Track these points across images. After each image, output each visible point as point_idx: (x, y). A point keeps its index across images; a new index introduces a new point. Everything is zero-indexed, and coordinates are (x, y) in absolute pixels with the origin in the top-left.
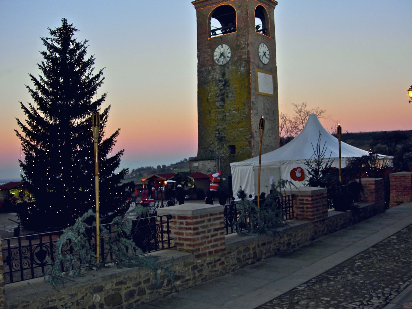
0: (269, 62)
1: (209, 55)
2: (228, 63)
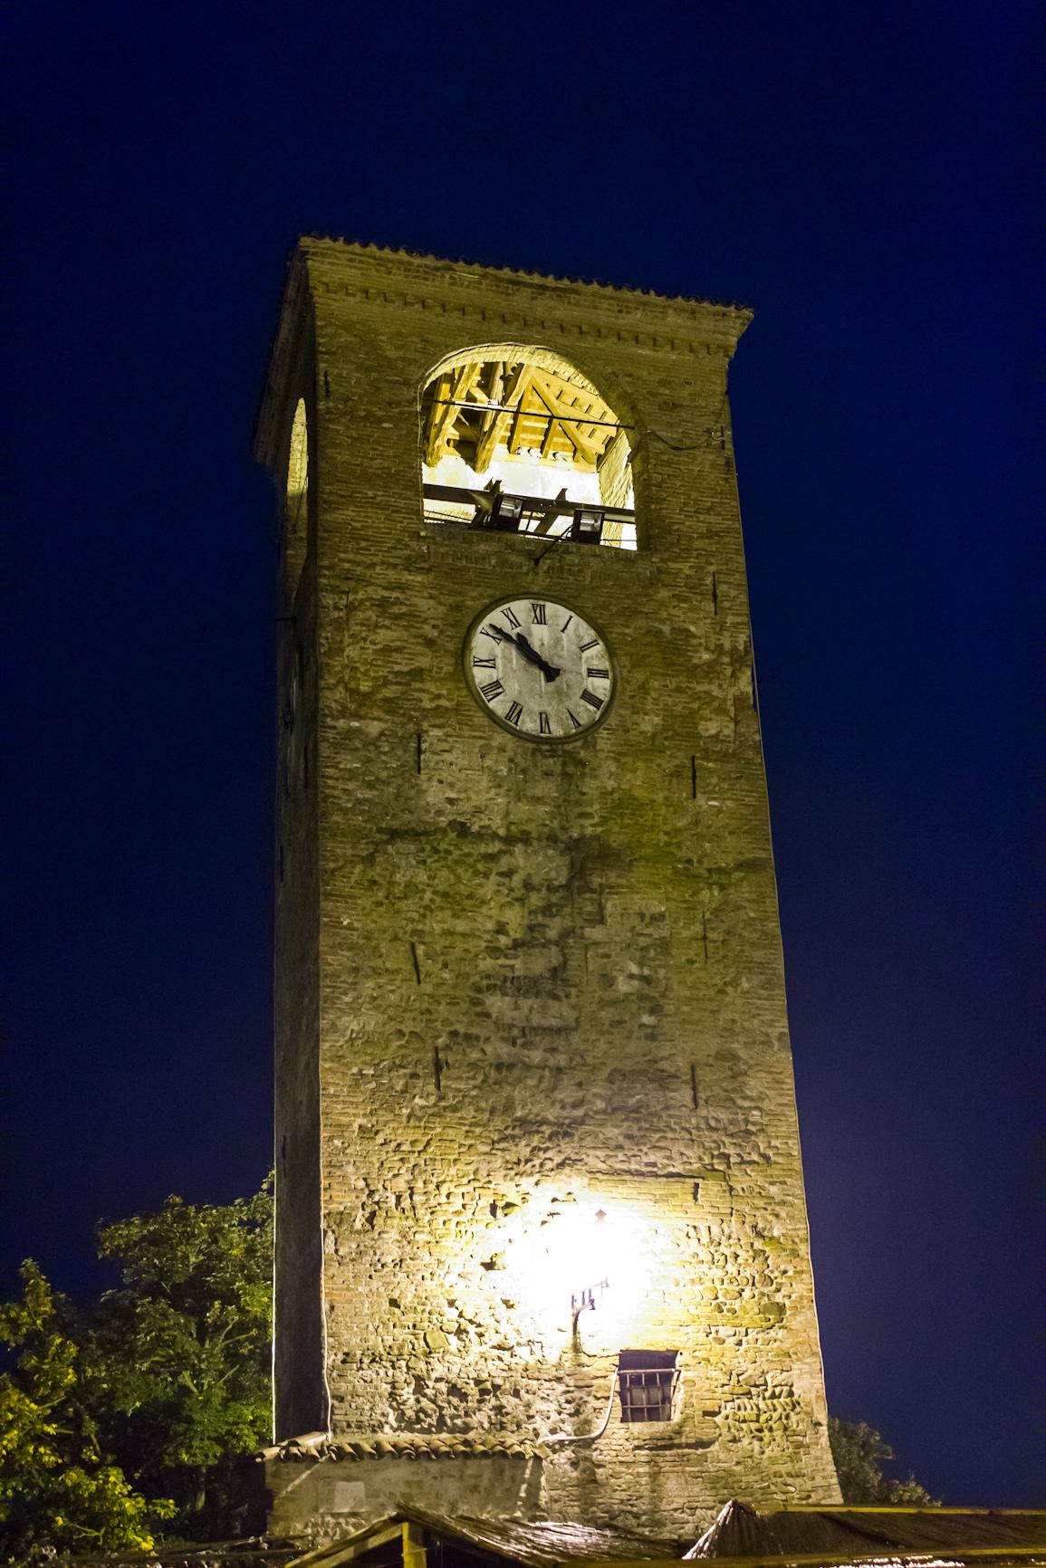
1: (430, 643)
2: (587, 733)
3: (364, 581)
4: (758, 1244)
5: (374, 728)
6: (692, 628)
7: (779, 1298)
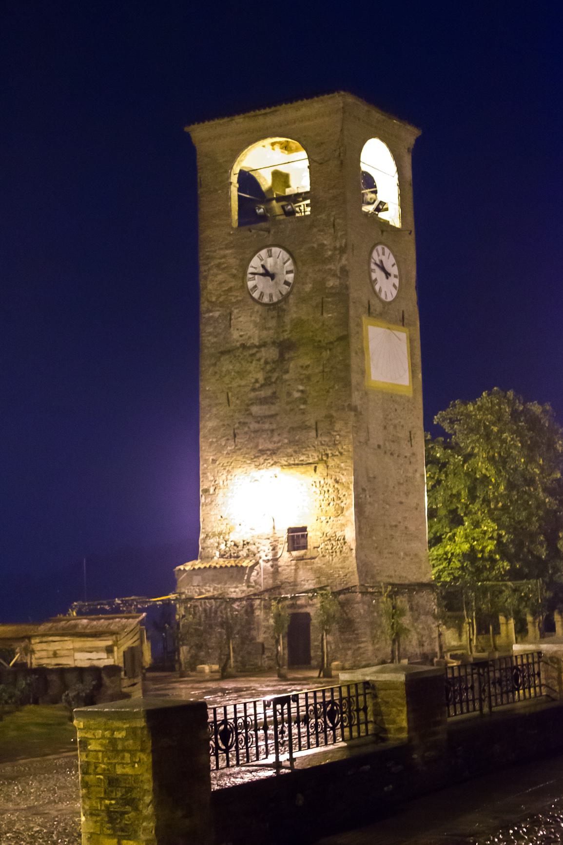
0: (397, 297)
1: (234, 276)
2: (285, 298)
3: (213, 258)
4: (336, 486)
5: (217, 314)
6: (325, 242)
7: (342, 505)
